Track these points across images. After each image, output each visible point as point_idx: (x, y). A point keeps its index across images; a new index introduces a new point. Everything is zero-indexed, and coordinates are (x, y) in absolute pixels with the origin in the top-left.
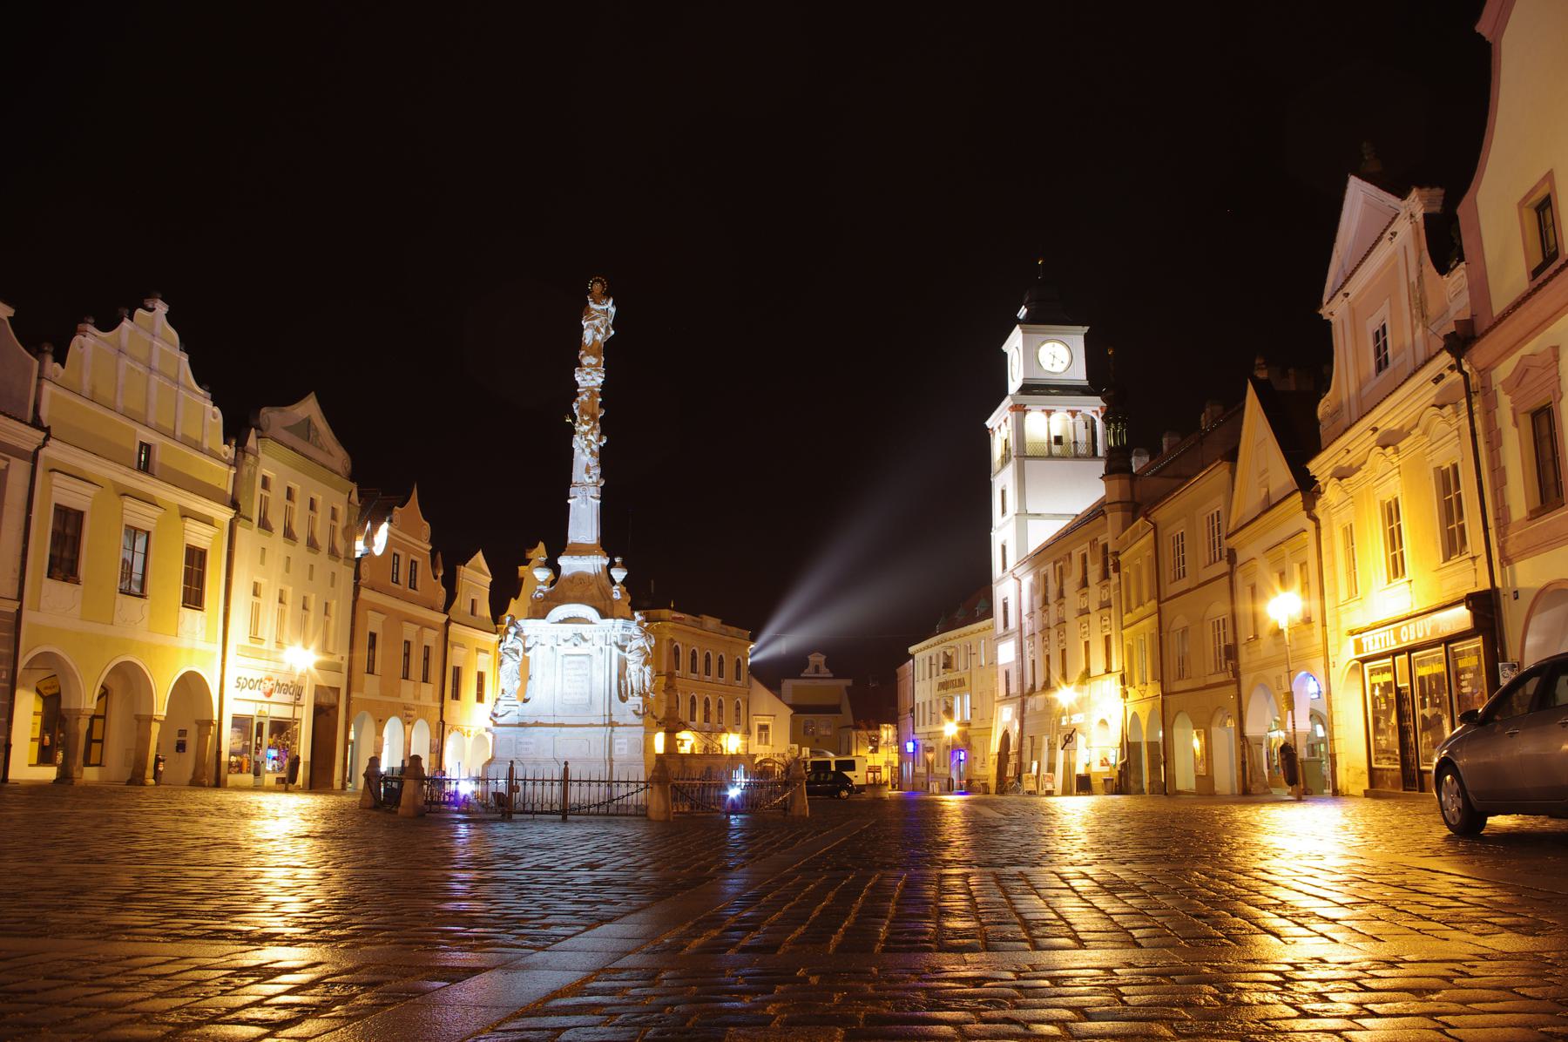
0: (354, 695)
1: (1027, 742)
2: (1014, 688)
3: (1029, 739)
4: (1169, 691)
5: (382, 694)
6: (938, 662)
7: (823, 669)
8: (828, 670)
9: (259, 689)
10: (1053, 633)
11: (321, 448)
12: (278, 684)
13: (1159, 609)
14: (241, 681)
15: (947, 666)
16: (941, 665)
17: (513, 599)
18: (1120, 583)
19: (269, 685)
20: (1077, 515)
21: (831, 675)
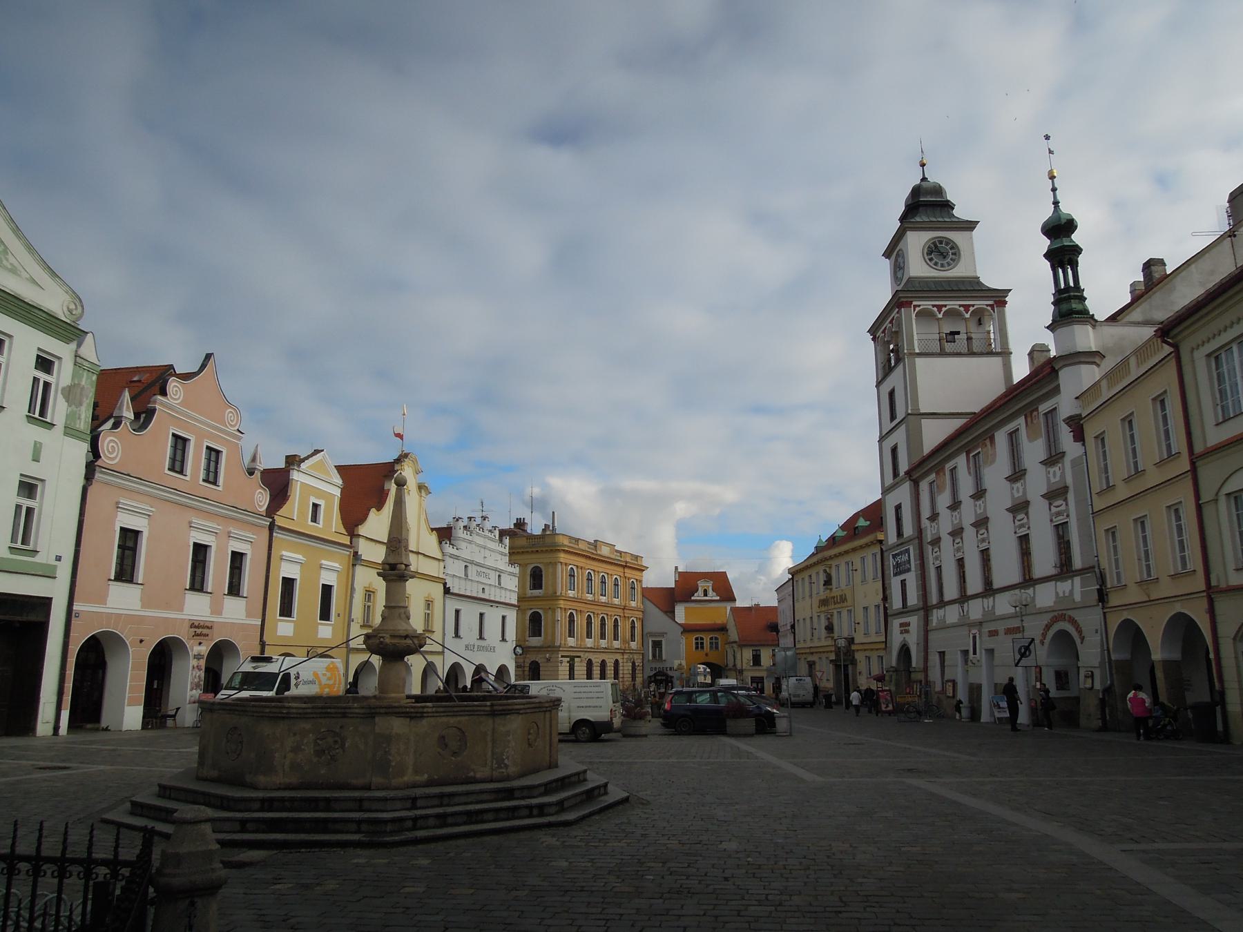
1: (934, 659)
2: (913, 599)
3: (937, 656)
4: (1223, 585)
5: (146, 603)
6: (818, 581)
7: (710, 592)
8: (715, 594)
10: (969, 533)
13: (1193, 464)
15: (828, 582)
16: (822, 583)
17: (373, 510)
18: (1086, 453)
20: (975, 413)
21: (718, 598)
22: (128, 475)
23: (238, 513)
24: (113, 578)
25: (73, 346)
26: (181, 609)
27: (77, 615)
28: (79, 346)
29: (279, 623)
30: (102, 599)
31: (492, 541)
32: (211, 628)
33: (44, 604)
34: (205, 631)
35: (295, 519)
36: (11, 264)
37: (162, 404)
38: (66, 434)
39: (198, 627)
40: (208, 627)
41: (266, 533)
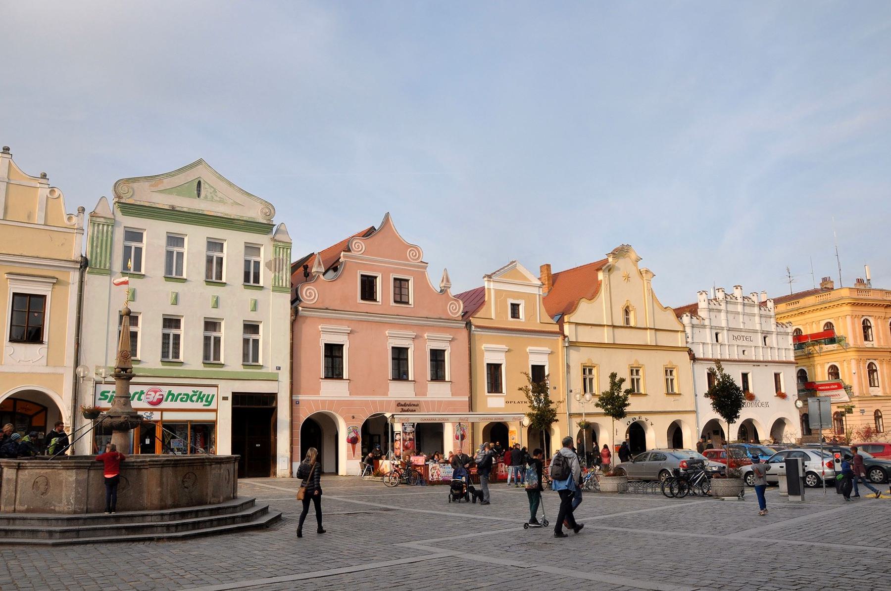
11: (222, 201)
12: (170, 393)
14: (109, 395)
19: (155, 397)
22: (327, 309)
23: (442, 322)
24: (324, 377)
26: (386, 394)
27: (297, 403)
29: (488, 398)
30: (317, 391)
31: (751, 306)
32: (418, 405)
33: (271, 398)
34: (411, 408)
35: (493, 317)
36: (220, 198)
38: (273, 291)
39: (405, 405)
40: (414, 405)
41: (465, 333)
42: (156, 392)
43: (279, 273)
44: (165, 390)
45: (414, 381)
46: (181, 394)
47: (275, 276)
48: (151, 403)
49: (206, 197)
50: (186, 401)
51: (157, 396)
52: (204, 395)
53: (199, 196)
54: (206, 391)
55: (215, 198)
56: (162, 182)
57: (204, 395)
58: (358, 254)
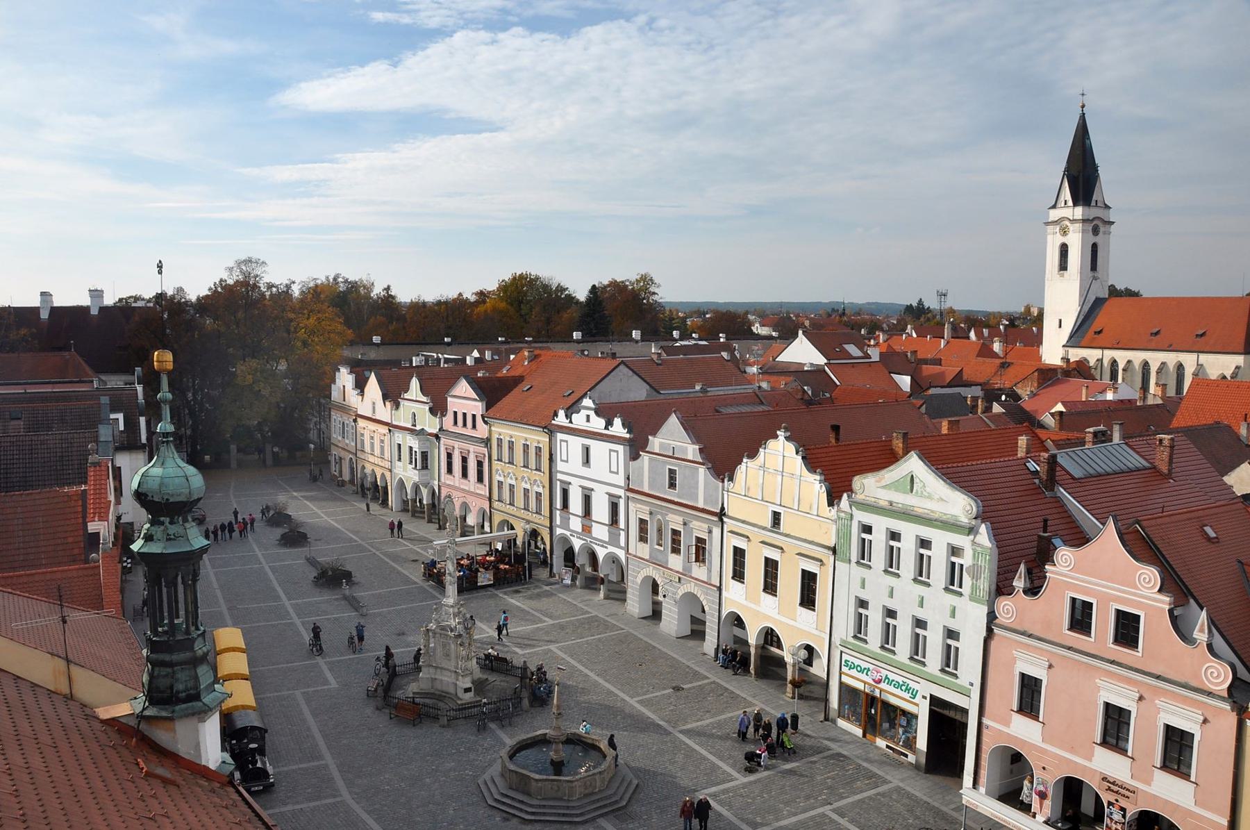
0: (985, 721)
9: (867, 674)
11: (930, 497)
12: (887, 677)
14: (850, 664)
25: (971, 537)
28: (975, 537)
30: (1007, 723)
37: (1052, 572)
42: (877, 672)
43: (977, 581)
44: (884, 673)
45: (1132, 758)
46: (893, 681)
47: (973, 584)
48: (874, 680)
49: (917, 492)
50: (897, 688)
51: (878, 677)
52: (911, 688)
53: (912, 491)
54: (912, 685)
55: (924, 493)
56: (884, 478)
57: (911, 688)
58: (1065, 570)
